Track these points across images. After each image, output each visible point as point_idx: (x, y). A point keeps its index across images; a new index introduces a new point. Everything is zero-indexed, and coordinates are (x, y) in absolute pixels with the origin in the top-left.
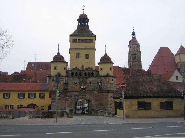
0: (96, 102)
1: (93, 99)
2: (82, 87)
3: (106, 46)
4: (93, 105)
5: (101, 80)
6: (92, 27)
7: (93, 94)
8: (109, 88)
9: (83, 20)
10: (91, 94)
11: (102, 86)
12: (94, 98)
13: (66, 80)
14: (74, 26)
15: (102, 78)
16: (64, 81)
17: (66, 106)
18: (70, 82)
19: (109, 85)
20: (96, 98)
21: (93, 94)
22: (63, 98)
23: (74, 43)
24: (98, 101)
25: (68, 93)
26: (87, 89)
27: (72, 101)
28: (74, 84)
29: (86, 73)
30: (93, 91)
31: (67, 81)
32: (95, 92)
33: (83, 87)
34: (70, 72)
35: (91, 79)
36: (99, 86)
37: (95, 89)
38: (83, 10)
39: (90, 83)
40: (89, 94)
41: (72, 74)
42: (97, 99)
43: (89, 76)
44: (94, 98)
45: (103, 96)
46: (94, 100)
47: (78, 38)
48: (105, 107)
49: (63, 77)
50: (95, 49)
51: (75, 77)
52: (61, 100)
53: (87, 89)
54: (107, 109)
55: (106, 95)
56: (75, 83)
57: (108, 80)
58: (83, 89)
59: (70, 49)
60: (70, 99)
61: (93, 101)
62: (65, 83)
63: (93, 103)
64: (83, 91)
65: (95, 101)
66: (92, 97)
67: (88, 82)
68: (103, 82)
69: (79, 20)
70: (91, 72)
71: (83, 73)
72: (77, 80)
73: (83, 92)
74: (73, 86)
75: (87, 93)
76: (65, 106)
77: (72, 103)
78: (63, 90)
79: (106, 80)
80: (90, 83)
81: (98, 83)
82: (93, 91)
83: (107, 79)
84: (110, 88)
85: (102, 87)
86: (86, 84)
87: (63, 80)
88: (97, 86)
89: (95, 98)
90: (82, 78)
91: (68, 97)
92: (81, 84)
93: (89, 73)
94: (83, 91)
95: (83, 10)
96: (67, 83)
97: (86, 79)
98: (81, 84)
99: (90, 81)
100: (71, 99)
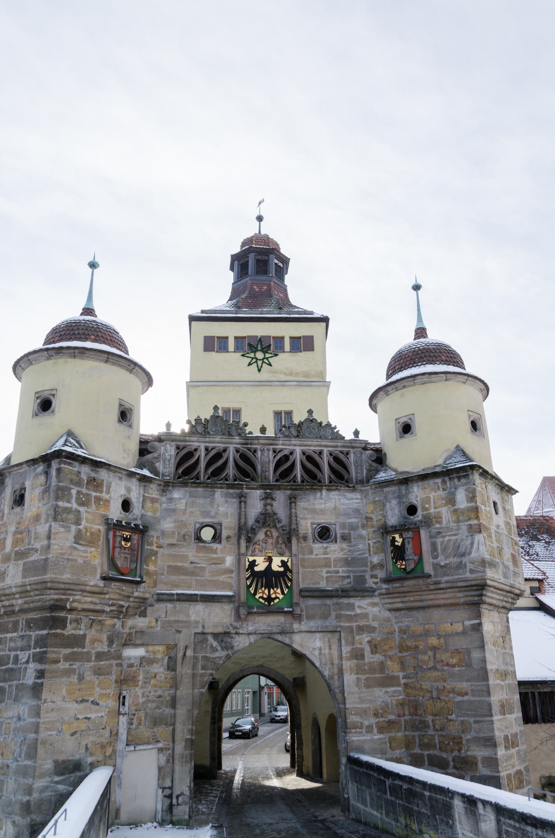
0: (381, 696)
1: (347, 664)
2: (261, 566)
3: (417, 288)
4: (352, 719)
5: (412, 510)
6: (301, 289)
7: (350, 618)
8: (483, 563)
9: (259, 266)
10: (331, 622)
11: (419, 551)
12: (358, 655)
13: (126, 505)
14: (217, 290)
15: (417, 494)
16: (115, 512)
17: (123, 735)
18: (168, 525)
19: (479, 538)
20: (378, 658)
21: (350, 618)
22: (100, 656)
23: (213, 354)
24: (389, 681)
25: (143, 614)
26: (303, 579)
27: (175, 685)
28: (199, 539)
29: (286, 458)
30: (344, 593)
31: (137, 510)
32: (362, 605)
33: (270, 560)
34: (169, 452)
35: (330, 505)
36: (399, 553)
37: (361, 579)
38: (260, 219)
39: (324, 533)
40: (313, 624)
41: (177, 468)
42: (382, 667)
43: (313, 479)
44: (358, 655)
45: (433, 641)
46: (359, 670)
47: (232, 331)
48: (458, 741)
49: (103, 474)
50: (327, 385)
51: (205, 485)
52: (68, 673)
53: (303, 579)
54: (479, 753)
55: (459, 628)
56: (207, 534)
57: (472, 498)
58: (269, 578)
59: (192, 385)
60: (159, 669)
61: (349, 679)
62: (118, 526)
63: (352, 702)
64: (269, 599)
65: (368, 686)
66: (346, 649)
67: (307, 525)
68: (427, 522)
69: (240, 263)
70: (325, 450)
71: (266, 461)
72: (222, 507)
73: (269, 608)
74: (191, 552)
75: (298, 618)
76: (115, 734)
77: (173, 703)
78: (94, 581)
79: (451, 500)
80: (324, 533)
81: (386, 530)
82: (344, 593)
83: (461, 496)
84: (492, 565)
85: (420, 561)
86: (289, 536)
87: (108, 501)
88: (376, 559)
89: (369, 657)
90: (259, 492)
91: (140, 652)
92: (249, 540)
93: (310, 458)
94: (269, 599)
95: (260, 219)
96: (142, 531)
97: (292, 500)
98: (246, 534)
99: (323, 520)
100: (171, 666)
